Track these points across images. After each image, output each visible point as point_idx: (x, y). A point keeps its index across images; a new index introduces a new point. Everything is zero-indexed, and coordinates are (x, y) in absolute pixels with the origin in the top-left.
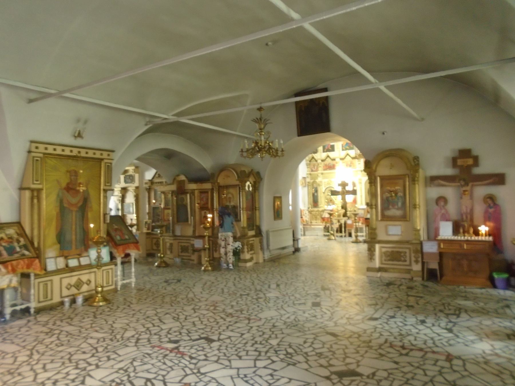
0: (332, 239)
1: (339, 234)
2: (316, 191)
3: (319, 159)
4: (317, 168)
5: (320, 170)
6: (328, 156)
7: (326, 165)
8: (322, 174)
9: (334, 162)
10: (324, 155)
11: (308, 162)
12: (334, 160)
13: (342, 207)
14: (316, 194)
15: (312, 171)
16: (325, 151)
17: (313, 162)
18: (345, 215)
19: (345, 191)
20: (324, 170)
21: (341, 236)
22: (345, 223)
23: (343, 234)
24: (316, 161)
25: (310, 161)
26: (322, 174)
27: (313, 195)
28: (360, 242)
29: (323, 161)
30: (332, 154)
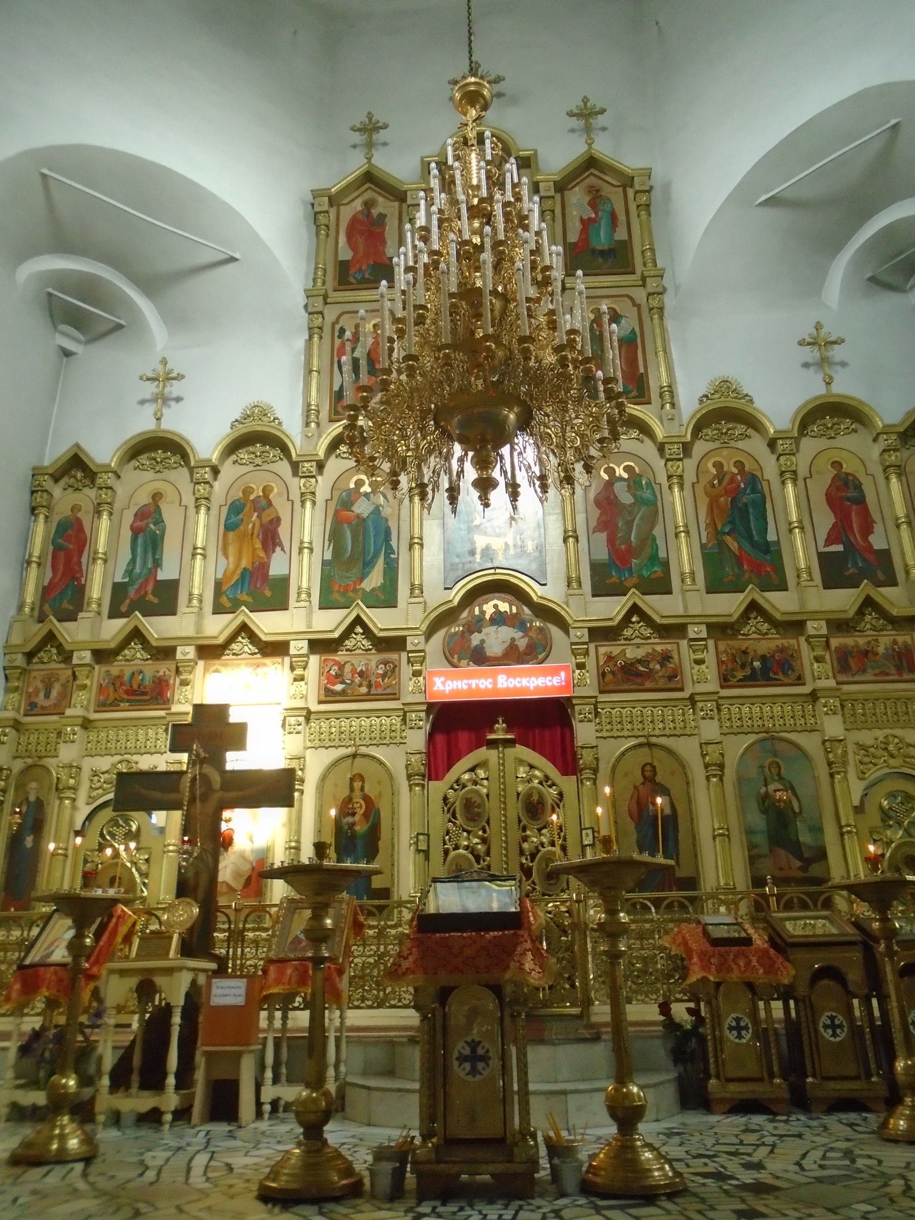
0: (62, 1159)
1: (144, 1102)
4: (65, 698)
5: (81, 704)
6: (137, 635)
7: (116, 681)
8: (86, 724)
9: (164, 668)
11: (20, 660)
12: (166, 652)
13: (183, 889)
14: (29, 841)
15: (32, 708)
16: (124, 608)
17: (50, 661)
18: (197, 942)
19: (216, 779)
20: (102, 706)
21: (152, 1118)
22: (194, 1001)
23: (171, 1100)
24: (66, 657)
25: (30, 656)
26: (86, 724)
27: (15, 841)
28: (355, 1191)
29: (101, 655)
30: (158, 628)
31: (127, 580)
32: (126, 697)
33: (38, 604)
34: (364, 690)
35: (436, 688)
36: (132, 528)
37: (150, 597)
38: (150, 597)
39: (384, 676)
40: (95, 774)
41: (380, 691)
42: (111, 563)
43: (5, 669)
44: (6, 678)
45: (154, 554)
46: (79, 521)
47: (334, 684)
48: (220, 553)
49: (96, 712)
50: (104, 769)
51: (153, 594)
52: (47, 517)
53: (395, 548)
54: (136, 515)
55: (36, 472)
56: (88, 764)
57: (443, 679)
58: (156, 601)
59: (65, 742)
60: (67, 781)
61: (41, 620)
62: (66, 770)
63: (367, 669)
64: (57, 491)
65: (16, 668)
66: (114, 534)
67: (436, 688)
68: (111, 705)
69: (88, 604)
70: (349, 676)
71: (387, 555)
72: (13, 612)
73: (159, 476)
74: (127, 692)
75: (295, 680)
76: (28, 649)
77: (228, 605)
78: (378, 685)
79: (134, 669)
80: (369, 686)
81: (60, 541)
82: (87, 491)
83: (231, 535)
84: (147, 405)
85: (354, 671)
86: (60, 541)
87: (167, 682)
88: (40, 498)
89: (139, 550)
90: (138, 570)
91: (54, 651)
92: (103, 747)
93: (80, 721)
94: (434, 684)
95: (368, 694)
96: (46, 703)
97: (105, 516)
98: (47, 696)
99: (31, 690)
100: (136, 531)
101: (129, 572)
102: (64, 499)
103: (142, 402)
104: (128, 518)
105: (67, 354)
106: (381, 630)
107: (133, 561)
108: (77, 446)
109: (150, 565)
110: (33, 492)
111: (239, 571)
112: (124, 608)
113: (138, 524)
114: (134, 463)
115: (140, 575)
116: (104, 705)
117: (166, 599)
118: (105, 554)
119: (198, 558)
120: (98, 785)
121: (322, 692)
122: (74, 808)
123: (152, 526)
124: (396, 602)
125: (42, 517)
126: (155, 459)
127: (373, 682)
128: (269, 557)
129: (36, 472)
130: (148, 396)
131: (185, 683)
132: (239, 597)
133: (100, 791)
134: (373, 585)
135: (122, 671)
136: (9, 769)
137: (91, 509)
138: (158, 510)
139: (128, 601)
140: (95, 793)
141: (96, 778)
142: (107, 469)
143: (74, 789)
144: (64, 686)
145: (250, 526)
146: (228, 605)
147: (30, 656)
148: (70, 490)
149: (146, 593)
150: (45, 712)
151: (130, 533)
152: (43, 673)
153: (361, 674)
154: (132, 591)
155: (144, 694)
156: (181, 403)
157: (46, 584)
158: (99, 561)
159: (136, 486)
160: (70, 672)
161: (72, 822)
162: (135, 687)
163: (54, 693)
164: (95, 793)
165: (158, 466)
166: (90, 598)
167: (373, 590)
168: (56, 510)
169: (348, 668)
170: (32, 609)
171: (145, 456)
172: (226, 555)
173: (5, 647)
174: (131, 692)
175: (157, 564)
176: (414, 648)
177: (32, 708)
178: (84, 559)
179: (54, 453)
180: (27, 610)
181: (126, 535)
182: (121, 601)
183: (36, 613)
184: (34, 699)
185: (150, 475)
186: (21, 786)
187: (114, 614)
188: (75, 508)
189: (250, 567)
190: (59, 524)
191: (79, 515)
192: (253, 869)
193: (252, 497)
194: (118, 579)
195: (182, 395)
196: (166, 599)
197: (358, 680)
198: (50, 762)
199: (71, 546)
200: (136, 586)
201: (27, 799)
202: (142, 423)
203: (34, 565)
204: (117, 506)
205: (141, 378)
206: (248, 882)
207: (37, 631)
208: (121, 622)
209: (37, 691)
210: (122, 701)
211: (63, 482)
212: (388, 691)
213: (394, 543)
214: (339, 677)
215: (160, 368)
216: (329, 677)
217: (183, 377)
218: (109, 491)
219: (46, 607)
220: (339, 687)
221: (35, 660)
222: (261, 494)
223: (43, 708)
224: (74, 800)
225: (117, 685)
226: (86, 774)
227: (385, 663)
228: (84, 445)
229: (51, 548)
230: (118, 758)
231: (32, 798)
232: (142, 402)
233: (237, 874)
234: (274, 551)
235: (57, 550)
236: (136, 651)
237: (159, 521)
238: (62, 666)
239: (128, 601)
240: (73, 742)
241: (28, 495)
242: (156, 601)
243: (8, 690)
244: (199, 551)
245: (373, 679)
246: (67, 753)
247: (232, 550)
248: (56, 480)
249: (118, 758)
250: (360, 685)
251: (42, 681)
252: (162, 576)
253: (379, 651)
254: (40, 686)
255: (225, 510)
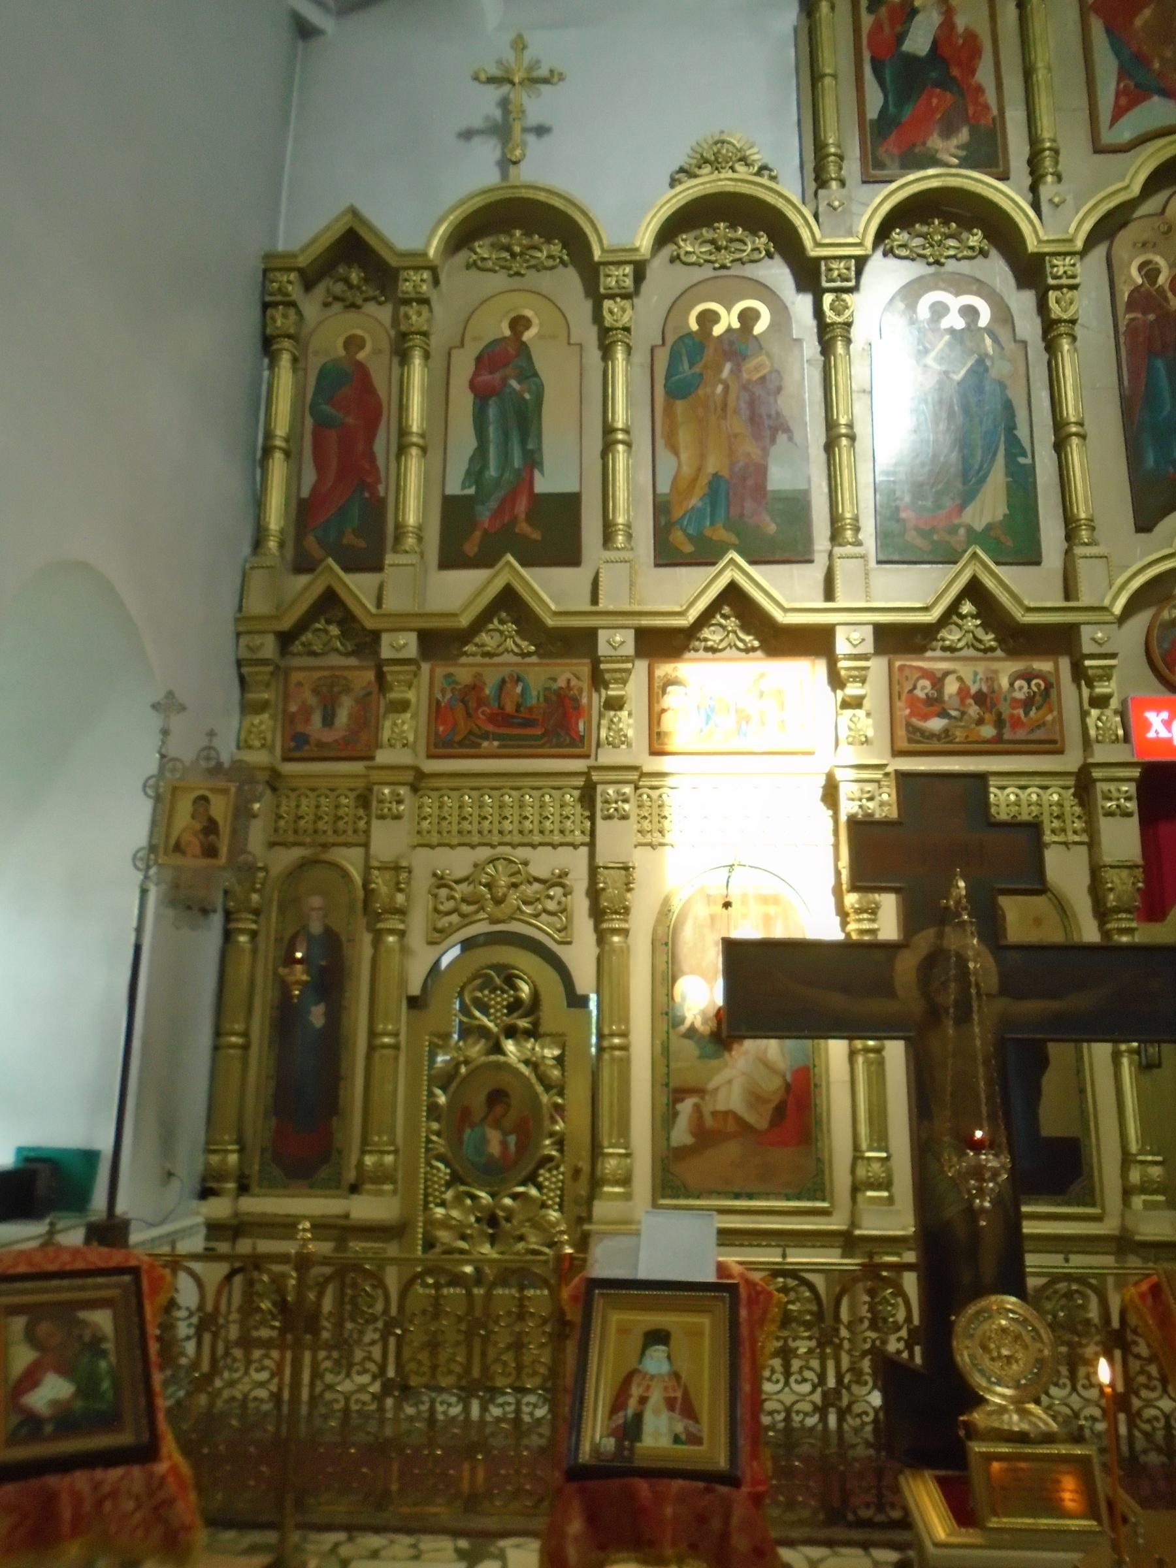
2: (330, 980)
3: (400, 622)
5: (403, 737)
6: (509, 602)
8: (418, 781)
9: (569, 673)
10: (460, 592)
11: (268, 647)
12: (578, 642)
14: (317, 1016)
15: (298, 746)
16: (471, 548)
20: (441, 746)
24: (365, 642)
25: (286, 639)
26: (418, 781)
29: (439, 642)
30: (553, 591)
31: (471, 491)
32: (491, 728)
33: (291, 532)
34: (988, 731)
35: (1151, 735)
36: (472, 385)
37: (524, 527)
38: (524, 527)
39: (1028, 703)
40: (440, 881)
41: (1021, 734)
42: (435, 453)
43: (239, 663)
44: (242, 680)
45: (523, 442)
46: (362, 371)
47: (925, 717)
48: (660, 442)
49: (430, 756)
50: (461, 873)
51: (529, 519)
52: (295, 360)
53: (1026, 443)
54: (479, 360)
55: (272, 265)
56: (424, 863)
57: (1165, 715)
58: (536, 536)
59: (382, 817)
60: (392, 898)
61: (303, 565)
62: (388, 875)
63: (993, 692)
64: (311, 307)
65: (264, 662)
66: (440, 394)
67: (1151, 735)
68: (461, 744)
69: (399, 537)
70: (956, 702)
71: (1010, 458)
72: (246, 549)
73: (516, 282)
74: (492, 719)
75: (845, 705)
76: (286, 624)
77: (688, 548)
78: (1016, 723)
79: (506, 671)
80: (999, 723)
81: (326, 408)
82: (370, 308)
83: (680, 406)
84: (477, 141)
85: (963, 692)
86: (326, 408)
87: (576, 700)
88: (281, 320)
89: (492, 431)
90: (492, 471)
91: (334, 630)
92: (455, 828)
93: (409, 776)
94: (1147, 725)
95: (998, 739)
96: (328, 736)
97: (417, 361)
98: (329, 720)
99: (293, 708)
100: (482, 394)
101: (475, 473)
102: (329, 328)
103: (467, 135)
104: (464, 366)
105: (304, 31)
106: (1029, 610)
107: (481, 452)
108: (354, 212)
109: (517, 463)
110: (266, 306)
111: (703, 481)
112: (471, 548)
113: (486, 377)
114: (463, 256)
115: (498, 482)
116: (448, 744)
117: (555, 531)
118: (422, 436)
119: (613, 448)
120: (450, 905)
121: (901, 733)
122: (405, 950)
123: (514, 383)
124: (1040, 555)
125: (285, 360)
126: (508, 248)
127: (1005, 715)
128: (765, 452)
129: (272, 265)
130: (477, 123)
131: (615, 704)
132: (708, 532)
133: (455, 918)
134: (987, 519)
135: (478, 676)
136: (265, 869)
137: (385, 345)
138: (523, 349)
139: (478, 534)
140: (443, 922)
141: (444, 892)
142: (418, 261)
143: (402, 912)
144: (364, 703)
145: (720, 389)
146: (688, 548)
147: (286, 639)
148: (337, 307)
149: (515, 519)
150: (325, 754)
151: (469, 398)
152: (317, 675)
153: (980, 698)
154: (484, 514)
155: (528, 723)
156: (547, 139)
157: (305, 493)
158: (414, 451)
159: (471, 304)
160: (370, 675)
161: (403, 982)
162: (510, 708)
163: (343, 717)
164: (443, 922)
165: (513, 263)
166: (399, 527)
167: (989, 527)
168: (315, 344)
169: (951, 687)
170: (282, 545)
171: (487, 241)
172: (675, 450)
173: (237, 620)
174: (501, 718)
175: (533, 461)
176: (1096, 650)
177: (298, 746)
178: (379, 447)
179: (304, 230)
180: (272, 544)
181: (463, 401)
182: (464, 535)
183: (289, 553)
184: (300, 728)
185: (499, 280)
186: (290, 904)
187: (451, 559)
188: (353, 343)
189: (725, 473)
190: (322, 375)
191: (361, 356)
192: (788, 1087)
193: (718, 330)
194: (454, 488)
195: (547, 122)
196: (555, 531)
197: (974, 710)
198: (350, 860)
199: (350, 420)
200: (493, 504)
201: (305, 928)
202: (475, 175)
203: (278, 456)
204: (437, 343)
205: (476, 78)
206: (780, 1112)
207: (302, 589)
208: (477, 576)
209: (306, 712)
210: (486, 736)
211: (320, 291)
212: (1039, 735)
213: (1022, 433)
214: (935, 704)
215: (510, 56)
216: (913, 702)
217: (561, 77)
218: (424, 309)
219: (311, 541)
220: (936, 724)
221: (297, 647)
222: (736, 325)
223: (321, 745)
224: (402, 934)
225: (472, 704)
226: (421, 883)
227: (1028, 676)
228: (369, 212)
229: (309, 422)
230: (484, 853)
231: (316, 928)
232: (467, 135)
233: (755, 1098)
234: (773, 440)
235: (322, 426)
236: (502, 638)
237: (529, 374)
238: (353, 661)
239: (478, 534)
240: (398, 817)
241: (255, 314)
242: (536, 536)
243: (248, 708)
244: (620, 436)
245: (1005, 709)
246: (387, 840)
247: (684, 436)
248: (308, 285)
249: (484, 853)
250: (980, 722)
251: (315, 691)
252: (543, 484)
253: (1013, 653)
254: (312, 700)
255: (663, 357)
